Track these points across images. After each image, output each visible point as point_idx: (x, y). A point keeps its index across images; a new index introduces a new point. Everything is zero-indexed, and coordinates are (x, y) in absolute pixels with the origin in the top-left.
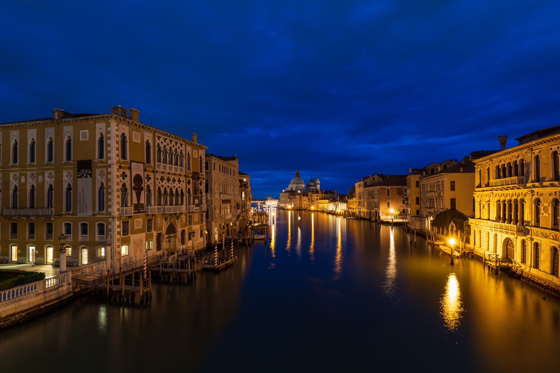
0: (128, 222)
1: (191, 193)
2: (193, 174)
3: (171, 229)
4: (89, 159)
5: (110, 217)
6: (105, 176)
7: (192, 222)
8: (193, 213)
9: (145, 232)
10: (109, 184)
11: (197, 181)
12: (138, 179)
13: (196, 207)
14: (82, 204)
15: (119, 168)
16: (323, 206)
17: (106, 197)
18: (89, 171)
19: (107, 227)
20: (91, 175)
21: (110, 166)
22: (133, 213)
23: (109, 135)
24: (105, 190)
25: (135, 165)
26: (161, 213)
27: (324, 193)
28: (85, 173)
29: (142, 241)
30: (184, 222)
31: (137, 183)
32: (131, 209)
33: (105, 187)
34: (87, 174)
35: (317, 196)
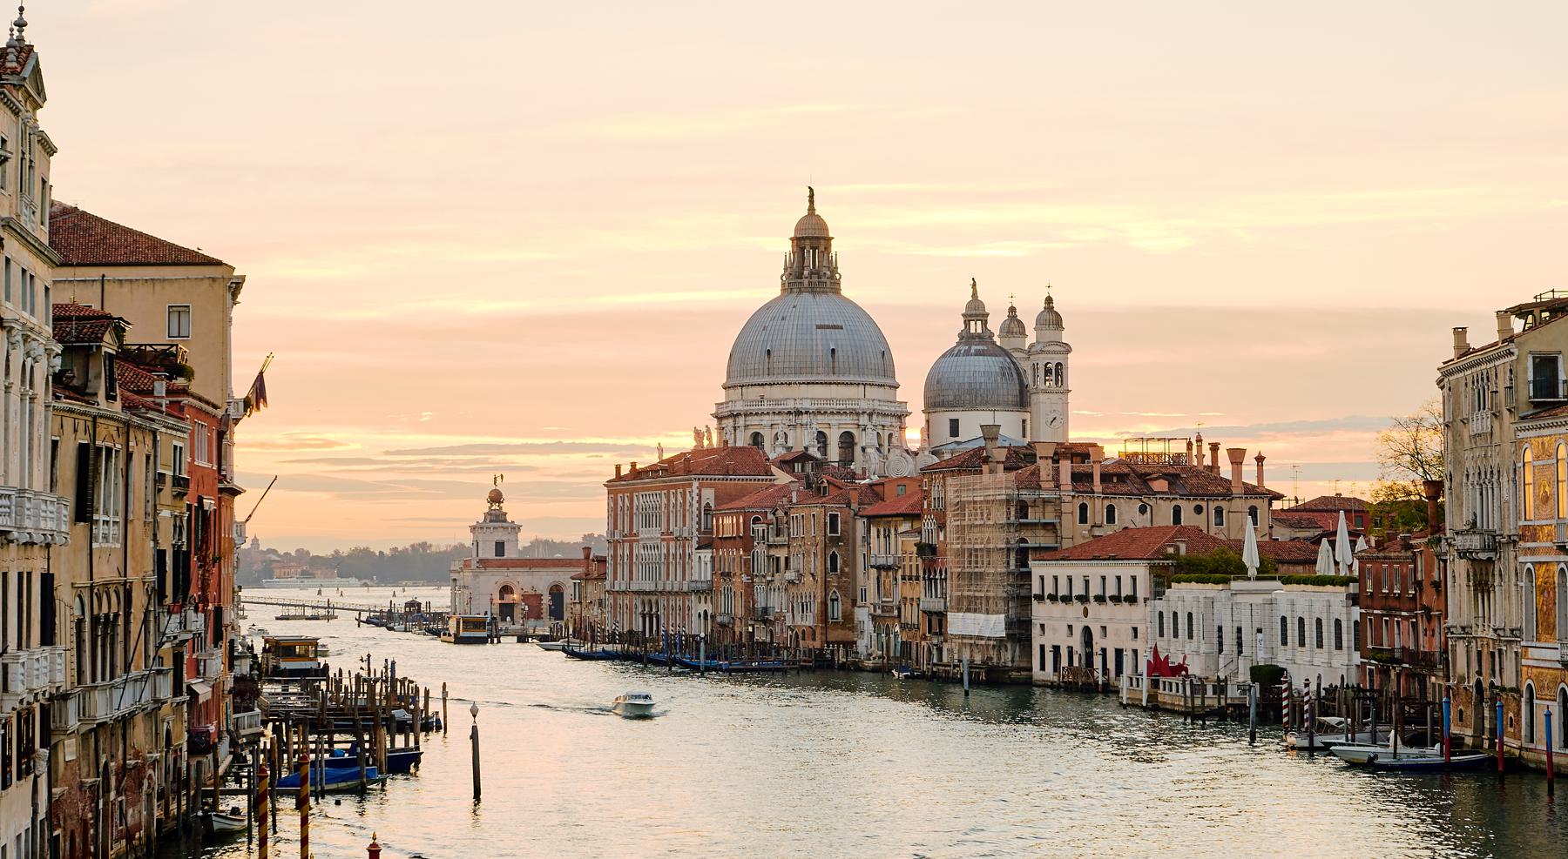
16: (1087, 632)
27: (1105, 478)
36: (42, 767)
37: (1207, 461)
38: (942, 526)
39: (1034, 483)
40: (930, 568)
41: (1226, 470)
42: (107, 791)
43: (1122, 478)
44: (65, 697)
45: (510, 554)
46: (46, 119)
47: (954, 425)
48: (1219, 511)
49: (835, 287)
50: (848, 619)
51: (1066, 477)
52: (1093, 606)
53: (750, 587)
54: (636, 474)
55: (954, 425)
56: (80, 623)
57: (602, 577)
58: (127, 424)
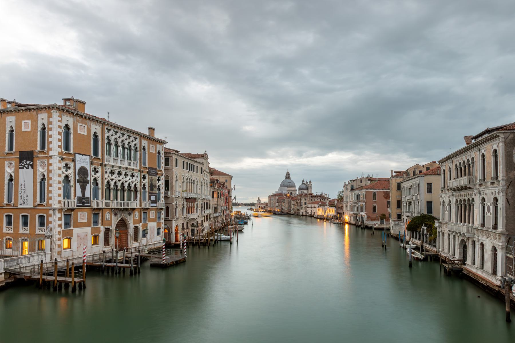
0: (70, 215)
1: (147, 189)
2: (149, 170)
3: (122, 225)
4: (31, 150)
5: (51, 209)
6: (47, 167)
7: (147, 219)
8: (149, 209)
9: (91, 226)
10: (51, 175)
11: (153, 177)
12: (83, 172)
13: (151, 203)
14: (23, 195)
15: (61, 159)
16: (312, 211)
17: (47, 189)
18: (30, 162)
19: (48, 219)
20: (32, 166)
21: (51, 157)
22: (76, 206)
23: (50, 126)
24: (46, 182)
25: (79, 158)
26: (109, 208)
28: (27, 164)
29: (87, 235)
30: (138, 218)
31: (82, 176)
32: (74, 203)
33: (46, 178)
34: (28, 165)
35: (306, 200)
36: (209, 220)
37: (324, 195)
38: (299, 201)
39: (307, 197)
40: (297, 205)
41: (325, 196)
42: (216, 223)
43: (315, 196)
44: (211, 214)
45: (260, 203)
46: (208, 161)
47: (301, 192)
48: (324, 200)
49: (290, 179)
50: (290, 210)
51: (310, 196)
52: (312, 208)
53: (281, 206)
54: (271, 196)
55: (301, 192)
56: (213, 207)
57: (268, 205)
58: (218, 189)
